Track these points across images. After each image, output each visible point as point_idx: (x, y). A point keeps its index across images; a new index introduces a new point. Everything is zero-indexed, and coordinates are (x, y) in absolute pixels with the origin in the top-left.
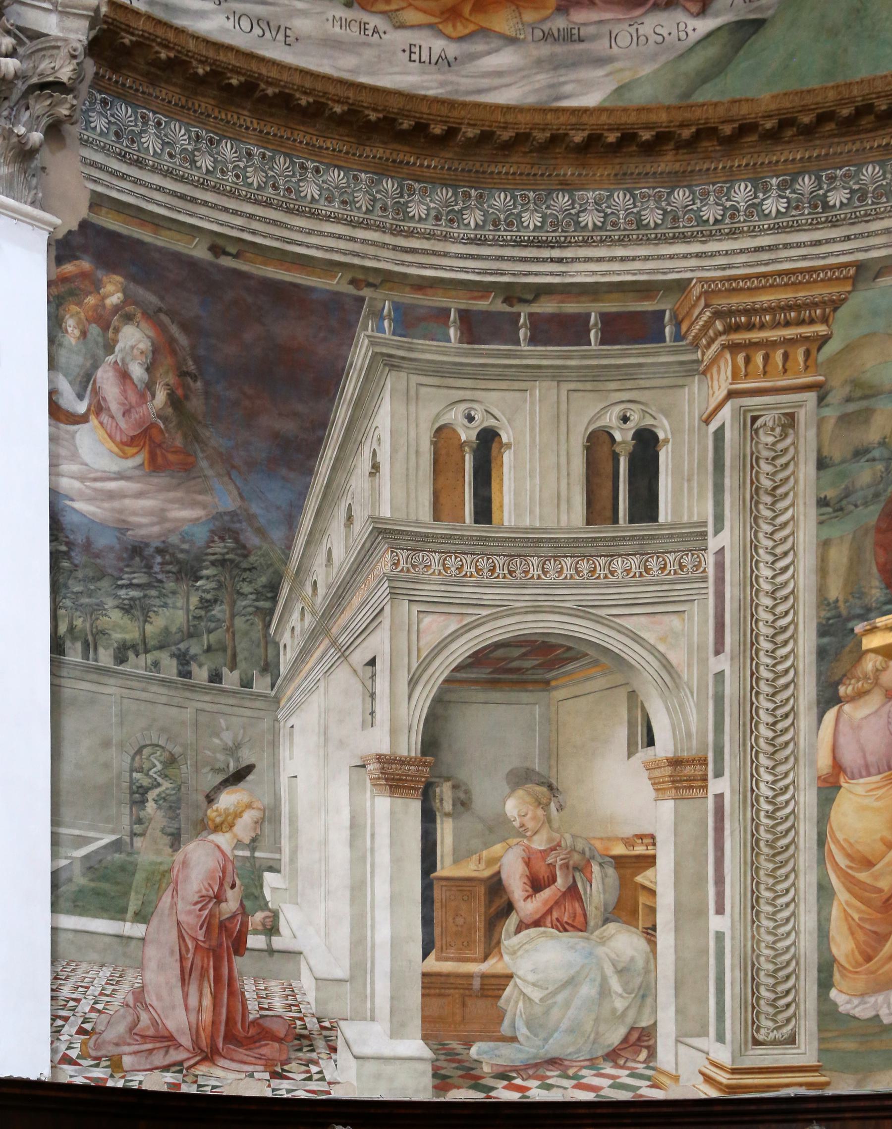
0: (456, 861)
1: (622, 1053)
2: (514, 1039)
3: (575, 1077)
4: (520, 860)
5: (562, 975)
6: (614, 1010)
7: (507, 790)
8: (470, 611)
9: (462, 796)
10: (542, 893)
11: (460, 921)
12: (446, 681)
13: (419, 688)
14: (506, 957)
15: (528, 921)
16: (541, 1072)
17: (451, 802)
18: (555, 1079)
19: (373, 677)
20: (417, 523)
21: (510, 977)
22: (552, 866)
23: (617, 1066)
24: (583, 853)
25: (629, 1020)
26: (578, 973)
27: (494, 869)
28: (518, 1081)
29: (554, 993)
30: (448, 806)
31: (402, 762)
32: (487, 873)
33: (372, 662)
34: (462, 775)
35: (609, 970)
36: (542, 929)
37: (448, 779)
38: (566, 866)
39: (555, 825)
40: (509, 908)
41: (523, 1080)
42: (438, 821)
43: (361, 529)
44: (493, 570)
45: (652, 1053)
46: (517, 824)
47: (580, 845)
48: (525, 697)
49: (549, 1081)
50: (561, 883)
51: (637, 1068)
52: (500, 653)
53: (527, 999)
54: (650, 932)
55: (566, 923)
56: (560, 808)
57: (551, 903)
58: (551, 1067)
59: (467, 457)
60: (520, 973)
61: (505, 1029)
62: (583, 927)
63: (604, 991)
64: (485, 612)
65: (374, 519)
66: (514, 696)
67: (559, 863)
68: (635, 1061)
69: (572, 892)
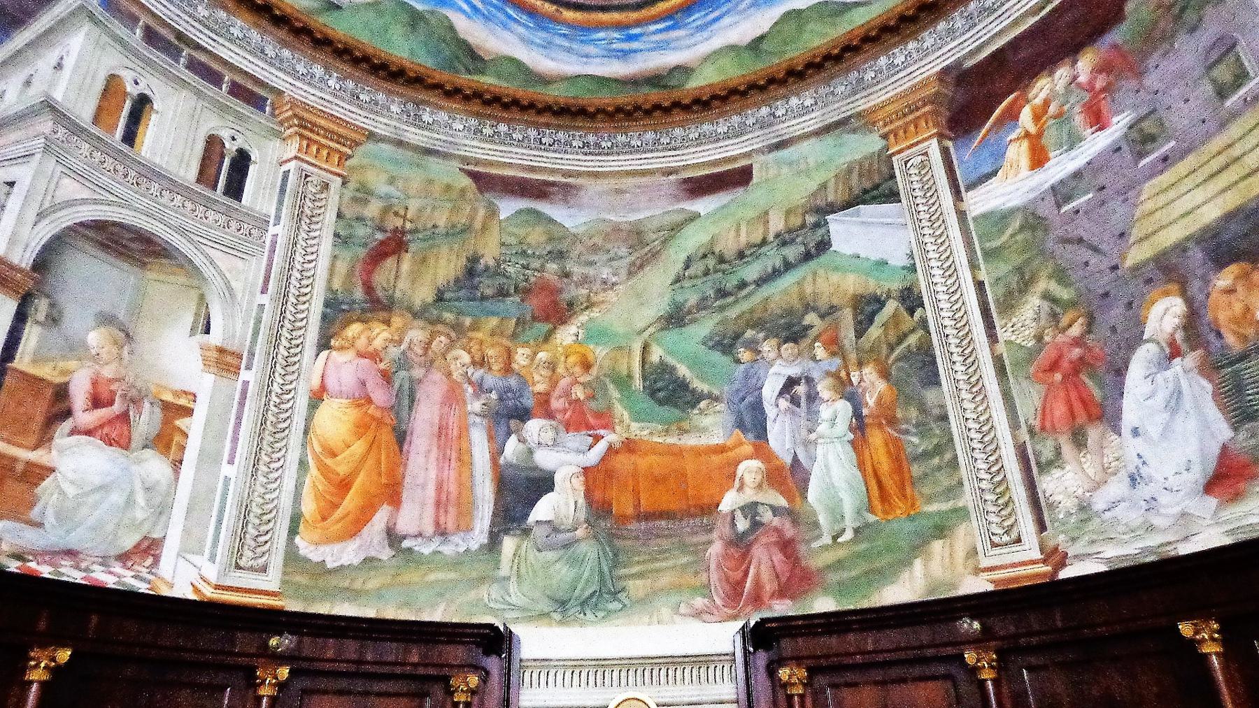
0: (35, 361)
1: (133, 556)
2: (39, 525)
3: (87, 570)
4: (88, 379)
5: (97, 481)
6: (134, 519)
7: (94, 324)
8: (102, 192)
9: (56, 315)
10: (99, 410)
11: (22, 410)
12: (69, 228)
13: (46, 221)
14: (54, 452)
15: (82, 426)
16: (57, 559)
17: (44, 314)
18: (68, 568)
19: (8, 194)
20: (81, 119)
21: (52, 470)
22: (113, 393)
23: (125, 566)
24: (140, 391)
25: (145, 530)
26: (113, 482)
27: (66, 379)
28: (33, 565)
29: (87, 494)
30: (41, 316)
31: (12, 267)
32: (59, 380)
33: (11, 184)
34: (62, 298)
35: (138, 486)
36: (92, 438)
37: (48, 296)
38: (125, 395)
39: (125, 362)
40: (68, 413)
41: (38, 564)
42: (29, 324)
43: (34, 95)
44: (126, 176)
45: (157, 559)
46: (93, 352)
47: (139, 384)
48: (126, 266)
49: (62, 570)
50: (117, 407)
51: (141, 572)
52: (115, 230)
53: (62, 493)
54: (177, 464)
55: (114, 439)
56: (131, 353)
57: (104, 420)
58: (66, 558)
59: (127, 102)
60: (61, 469)
61: (35, 514)
62: (125, 446)
63: (130, 502)
64: (115, 199)
65: (48, 96)
66: (119, 262)
67: (119, 393)
68: (140, 564)
69: (124, 417)
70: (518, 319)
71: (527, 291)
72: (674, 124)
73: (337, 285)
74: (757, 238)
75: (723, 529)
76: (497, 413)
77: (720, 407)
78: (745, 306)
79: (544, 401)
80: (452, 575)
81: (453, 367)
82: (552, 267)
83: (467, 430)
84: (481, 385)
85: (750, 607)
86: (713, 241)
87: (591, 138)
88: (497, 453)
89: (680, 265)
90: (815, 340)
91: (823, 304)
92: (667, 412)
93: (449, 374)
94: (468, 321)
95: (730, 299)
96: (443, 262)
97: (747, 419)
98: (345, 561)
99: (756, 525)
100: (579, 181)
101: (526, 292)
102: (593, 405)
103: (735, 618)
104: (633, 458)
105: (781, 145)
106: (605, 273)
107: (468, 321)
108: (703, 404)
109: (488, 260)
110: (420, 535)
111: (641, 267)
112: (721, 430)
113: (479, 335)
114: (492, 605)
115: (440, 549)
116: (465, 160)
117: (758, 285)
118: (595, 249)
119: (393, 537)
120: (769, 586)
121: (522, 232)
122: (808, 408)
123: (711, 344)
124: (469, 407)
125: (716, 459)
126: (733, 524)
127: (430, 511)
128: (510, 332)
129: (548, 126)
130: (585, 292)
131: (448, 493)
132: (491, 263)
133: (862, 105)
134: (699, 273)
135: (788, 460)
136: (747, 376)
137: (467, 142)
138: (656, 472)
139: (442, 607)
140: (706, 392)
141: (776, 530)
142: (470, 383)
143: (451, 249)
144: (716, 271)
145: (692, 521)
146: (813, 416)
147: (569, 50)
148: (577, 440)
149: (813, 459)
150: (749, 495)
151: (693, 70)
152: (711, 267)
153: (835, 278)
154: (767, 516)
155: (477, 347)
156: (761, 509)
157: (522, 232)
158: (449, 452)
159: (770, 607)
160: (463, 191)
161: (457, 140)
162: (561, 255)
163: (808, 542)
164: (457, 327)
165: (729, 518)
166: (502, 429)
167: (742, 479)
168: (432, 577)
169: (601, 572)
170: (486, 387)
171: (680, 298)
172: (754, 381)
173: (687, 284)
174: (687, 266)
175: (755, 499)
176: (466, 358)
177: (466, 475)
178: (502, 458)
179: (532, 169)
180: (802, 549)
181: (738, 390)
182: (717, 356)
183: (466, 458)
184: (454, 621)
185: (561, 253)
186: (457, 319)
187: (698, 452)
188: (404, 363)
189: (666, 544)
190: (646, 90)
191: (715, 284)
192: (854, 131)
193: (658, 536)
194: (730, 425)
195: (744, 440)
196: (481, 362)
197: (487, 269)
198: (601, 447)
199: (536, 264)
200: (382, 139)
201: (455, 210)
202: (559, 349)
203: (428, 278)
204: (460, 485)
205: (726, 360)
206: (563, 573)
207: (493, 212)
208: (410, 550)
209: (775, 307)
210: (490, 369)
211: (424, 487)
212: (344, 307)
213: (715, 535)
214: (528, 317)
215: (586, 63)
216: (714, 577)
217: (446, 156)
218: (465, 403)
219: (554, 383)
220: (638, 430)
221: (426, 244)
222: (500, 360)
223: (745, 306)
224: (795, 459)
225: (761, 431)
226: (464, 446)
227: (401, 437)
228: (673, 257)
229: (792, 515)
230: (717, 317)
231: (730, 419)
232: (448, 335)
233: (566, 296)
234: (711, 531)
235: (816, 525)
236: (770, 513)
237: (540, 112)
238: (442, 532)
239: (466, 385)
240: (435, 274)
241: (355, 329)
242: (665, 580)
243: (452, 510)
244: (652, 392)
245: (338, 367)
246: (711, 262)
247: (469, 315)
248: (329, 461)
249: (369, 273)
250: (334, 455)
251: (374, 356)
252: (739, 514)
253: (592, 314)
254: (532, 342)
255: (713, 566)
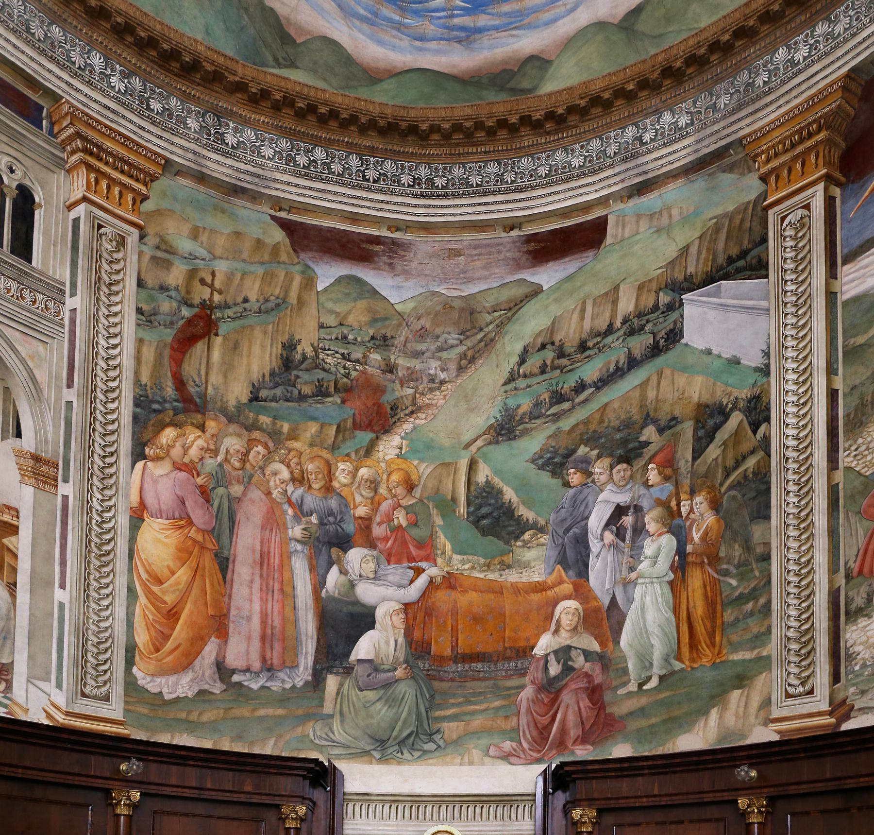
70: (339, 426)
71: (348, 390)
72: (522, 152)
73: (145, 379)
74: (602, 324)
75: (535, 673)
76: (318, 539)
77: (544, 539)
78: (581, 414)
79: (366, 524)
80: (280, 712)
81: (272, 484)
82: (375, 357)
83: (289, 558)
84: (301, 505)
85: (554, 752)
86: (552, 330)
87: (423, 171)
88: (319, 585)
89: (516, 359)
90: (650, 461)
91: (663, 417)
92: (492, 543)
93: (269, 493)
94: (286, 427)
95: (566, 405)
96: (256, 349)
97: (570, 554)
98: (181, 692)
99: (568, 669)
100: (408, 237)
101: (346, 391)
102: (415, 533)
103: (538, 761)
104: (453, 594)
105: (642, 189)
106: (433, 367)
107: (286, 427)
108: (527, 536)
109: (305, 348)
110: (248, 670)
111: (472, 360)
112: (543, 566)
113: (297, 445)
114: (317, 741)
115: (268, 684)
116: (277, 203)
117: (598, 389)
118: (422, 334)
119: (222, 670)
120: (574, 732)
121: (341, 308)
122: (633, 541)
123: (540, 462)
124: (290, 531)
125: (535, 597)
126: (546, 669)
127: (256, 644)
128: (330, 441)
129: (373, 151)
130: (410, 391)
131: (273, 628)
132: (309, 351)
133: (746, 128)
134: (536, 370)
135: (606, 601)
136: (575, 502)
137: (278, 176)
138: (475, 610)
139: (272, 742)
140: (531, 520)
141: (587, 675)
142: (289, 502)
143: (265, 333)
144: (554, 368)
145: (506, 665)
146: (636, 553)
147: (399, 27)
148: (396, 572)
149: (630, 601)
150: (564, 638)
151: (549, 62)
152: (549, 362)
153: (681, 380)
154: (579, 661)
155: (295, 460)
156: (573, 653)
157: (341, 308)
158: (271, 582)
159: (573, 753)
160: (276, 249)
161: (267, 174)
162: (383, 342)
163: (617, 688)
164: (275, 435)
165: (542, 663)
166: (323, 558)
167: (558, 621)
168: (262, 712)
169: (419, 715)
170: (305, 508)
171: (511, 403)
172: (582, 508)
173: (521, 383)
174: (522, 361)
175: (568, 642)
176: (285, 474)
177: (288, 610)
178: (324, 591)
179: (354, 218)
180: (608, 697)
181: (565, 520)
182: (545, 478)
183: (287, 589)
184: (283, 755)
185: (385, 338)
186: (274, 424)
187: (517, 590)
188: (221, 478)
189: (480, 686)
190: (491, 96)
191: (551, 385)
192: (730, 169)
193: (474, 679)
194: (552, 561)
195: (565, 578)
196: (299, 479)
197: (304, 358)
198: (422, 580)
199: (357, 354)
200: (181, 171)
201: (268, 278)
202: (382, 464)
203: (241, 370)
204: (284, 619)
205: (556, 482)
206: (382, 713)
207: (309, 282)
208: (239, 684)
209: (613, 418)
210: (310, 487)
211: (249, 619)
212: (156, 406)
213: (527, 679)
214: (349, 423)
215: (421, 49)
216: (524, 720)
217: (255, 197)
218: (287, 529)
219: (375, 503)
220: (459, 564)
221: (238, 323)
222: (320, 476)
223: (581, 414)
224: (613, 600)
225: (583, 571)
226: (286, 575)
227: (224, 564)
228: (508, 349)
229: (603, 660)
230: (552, 428)
231: (554, 554)
232: (266, 446)
233: (387, 399)
234: (524, 675)
235: (625, 671)
236: (582, 659)
237: (363, 130)
238: (269, 668)
239: (286, 507)
240: (249, 365)
241: (169, 434)
242: (477, 722)
243: (277, 646)
244: (476, 520)
245: (155, 482)
246: (549, 355)
247: (288, 421)
248: (155, 589)
249: (178, 361)
250: (160, 582)
251: (190, 468)
252: (552, 659)
253: (417, 422)
254: (353, 456)
255: (523, 710)
